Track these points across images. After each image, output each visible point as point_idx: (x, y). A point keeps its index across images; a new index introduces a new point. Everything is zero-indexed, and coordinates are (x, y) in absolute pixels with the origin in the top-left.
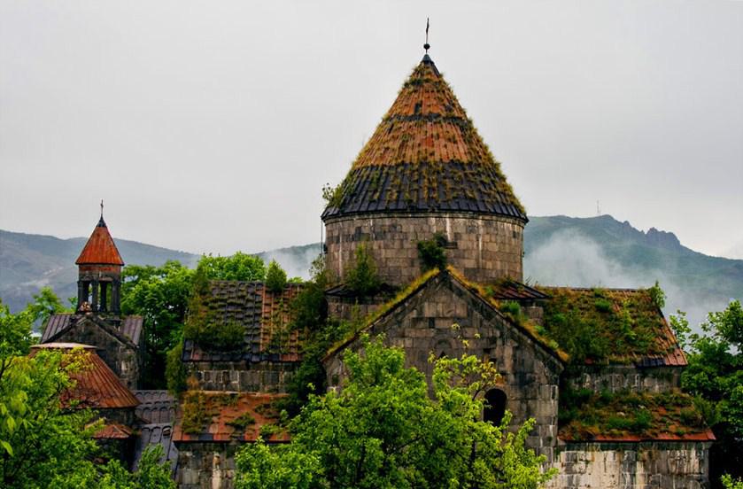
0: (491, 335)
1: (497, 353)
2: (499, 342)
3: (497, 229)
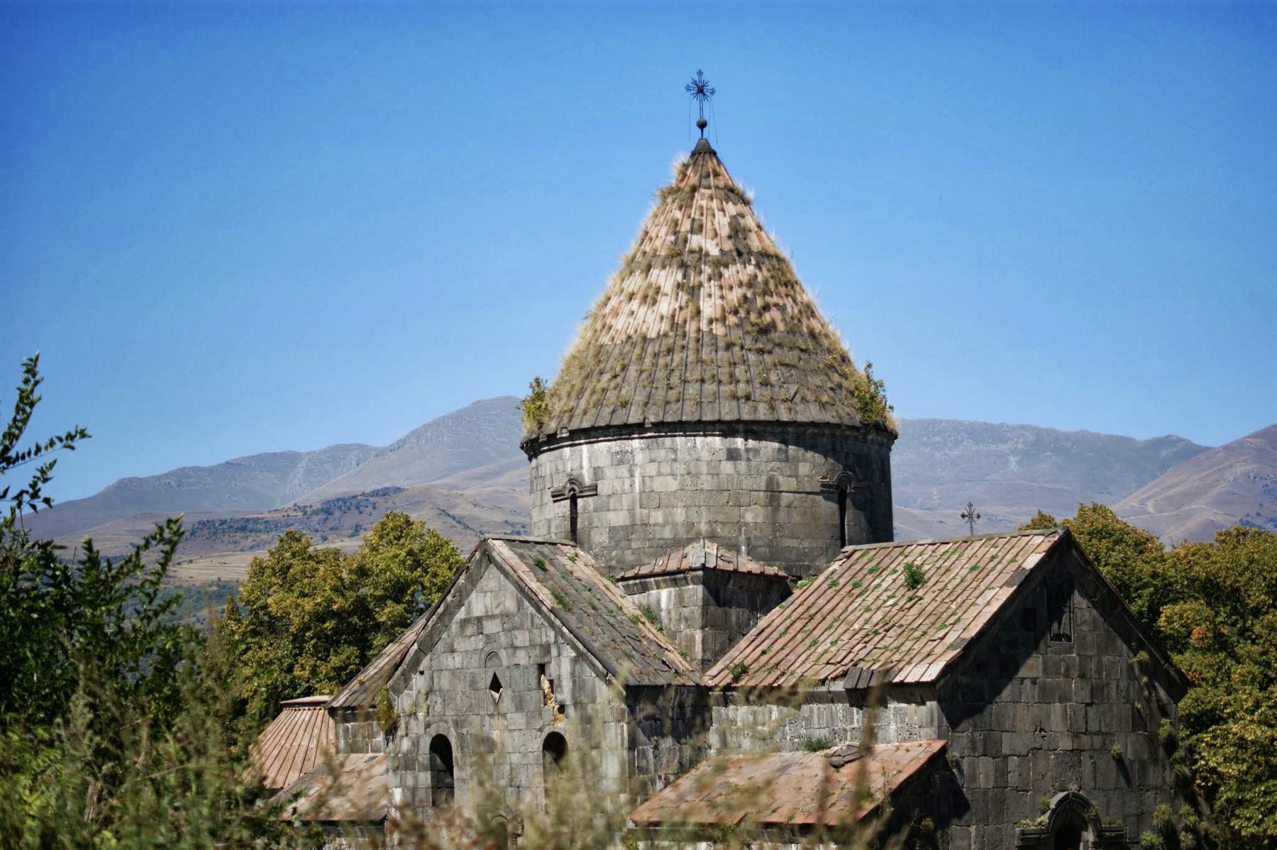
0: (544, 640)
1: (552, 669)
2: (554, 652)
3: (674, 451)
